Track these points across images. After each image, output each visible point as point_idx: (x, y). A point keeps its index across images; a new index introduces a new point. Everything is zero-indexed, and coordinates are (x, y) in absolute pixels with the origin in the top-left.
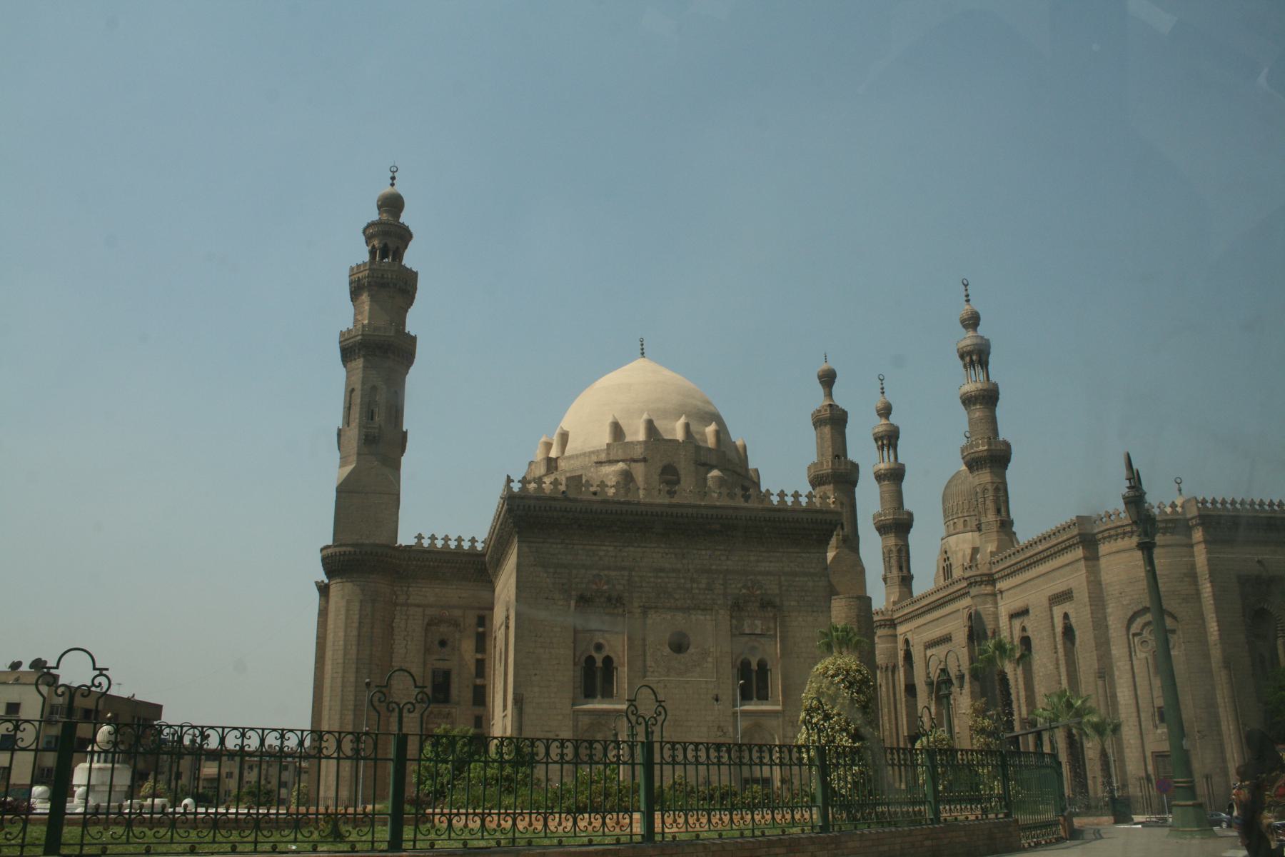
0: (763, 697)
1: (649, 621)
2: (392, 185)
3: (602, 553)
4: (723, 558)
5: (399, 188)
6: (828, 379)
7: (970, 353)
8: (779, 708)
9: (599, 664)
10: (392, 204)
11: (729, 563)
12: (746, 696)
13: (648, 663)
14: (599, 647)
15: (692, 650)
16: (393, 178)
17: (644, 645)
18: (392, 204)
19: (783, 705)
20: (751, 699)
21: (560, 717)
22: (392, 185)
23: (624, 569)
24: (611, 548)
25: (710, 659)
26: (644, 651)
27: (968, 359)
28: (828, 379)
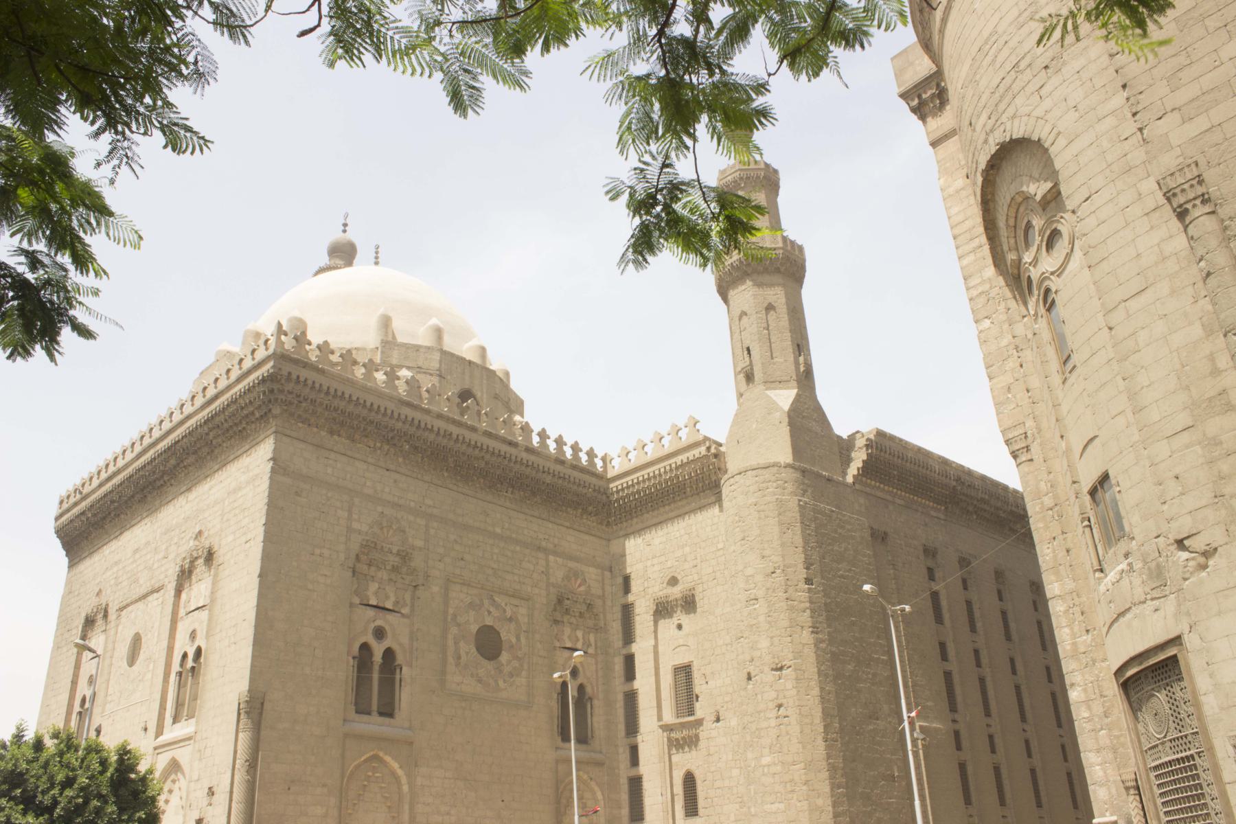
1: (120, 628)
2: (345, 231)
5: (351, 235)
22: (345, 231)
23: (116, 563)
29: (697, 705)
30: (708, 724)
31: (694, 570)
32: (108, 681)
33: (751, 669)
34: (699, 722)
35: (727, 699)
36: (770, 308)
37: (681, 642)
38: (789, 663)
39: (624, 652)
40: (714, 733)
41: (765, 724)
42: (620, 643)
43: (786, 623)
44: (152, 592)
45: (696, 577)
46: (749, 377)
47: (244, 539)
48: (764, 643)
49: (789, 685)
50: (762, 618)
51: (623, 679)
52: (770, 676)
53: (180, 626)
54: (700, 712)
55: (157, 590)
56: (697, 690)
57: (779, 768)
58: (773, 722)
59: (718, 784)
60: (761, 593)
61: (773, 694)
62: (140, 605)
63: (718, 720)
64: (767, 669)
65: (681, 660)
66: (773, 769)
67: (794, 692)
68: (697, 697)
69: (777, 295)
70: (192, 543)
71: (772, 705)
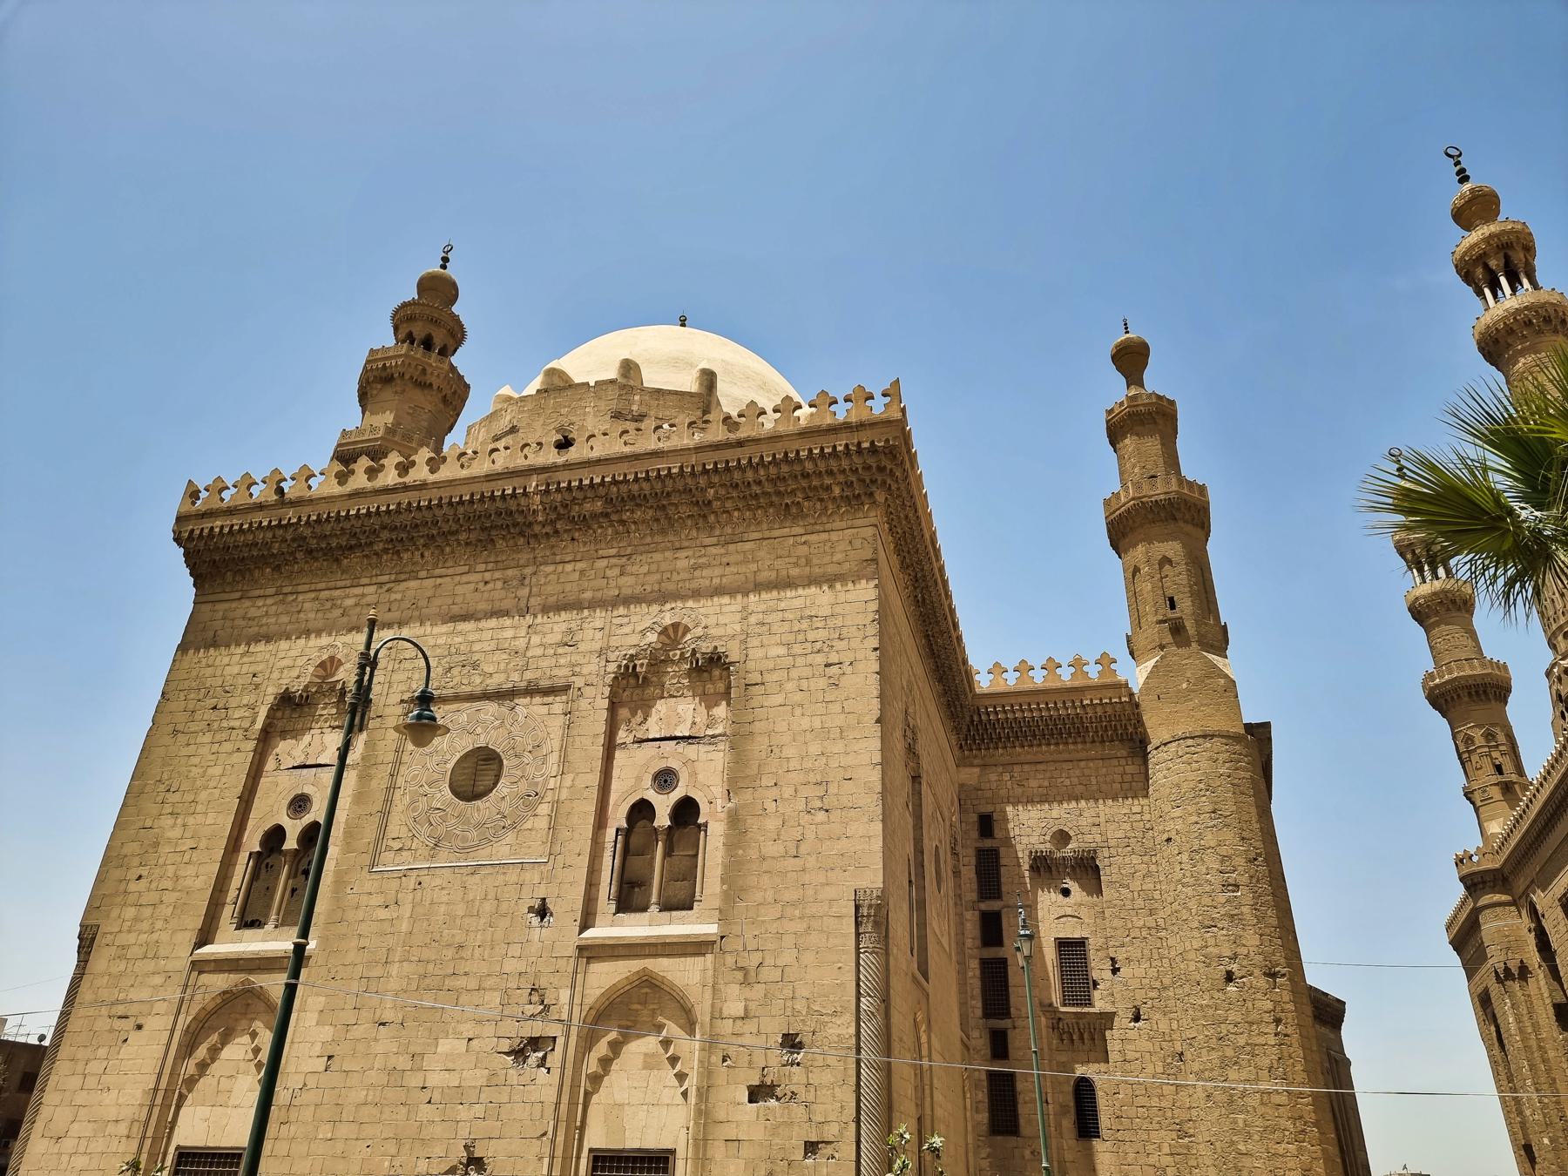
0: (680, 903)
2: (444, 267)
3: (349, 602)
4: (616, 571)
5: (452, 271)
6: (1131, 359)
7: (1481, 259)
8: (711, 929)
9: (291, 843)
10: (438, 290)
11: (627, 581)
12: (629, 899)
13: (393, 830)
14: (300, 803)
15: (503, 787)
16: (445, 260)
17: (391, 788)
18: (438, 290)
19: (724, 917)
20: (644, 909)
21: (158, 980)
22: (444, 267)
24: (372, 589)
25: (544, 809)
26: (388, 801)
27: (1479, 272)
28: (1131, 359)
29: (1096, 994)
30: (1122, 1021)
31: (1094, 829)
32: (385, 814)
33: (1234, 967)
34: (1108, 1019)
35: (1154, 994)
36: (1166, 561)
37: (1069, 911)
38: (1284, 971)
39: (983, 906)
40: (1131, 1034)
41: (1261, 1040)
42: (974, 896)
43: (1274, 922)
44: (531, 691)
45: (1098, 838)
46: (1177, 629)
47: (820, 659)
48: (1251, 939)
49: (1287, 996)
50: (1245, 909)
51: (978, 942)
52: (1262, 982)
53: (619, 755)
54: (1100, 1004)
55: (552, 691)
56: (1095, 975)
57: (1283, 1099)
58: (1272, 1040)
59: (1141, 1101)
60: (1244, 879)
61: (1269, 1005)
62: (491, 708)
63: (1137, 1018)
64: (1257, 972)
65: (1072, 931)
66: (1276, 1099)
67: (1291, 1007)
68: (1095, 984)
69: (1173, 549)
70: (652, 637)
71: (1268, 1018)
